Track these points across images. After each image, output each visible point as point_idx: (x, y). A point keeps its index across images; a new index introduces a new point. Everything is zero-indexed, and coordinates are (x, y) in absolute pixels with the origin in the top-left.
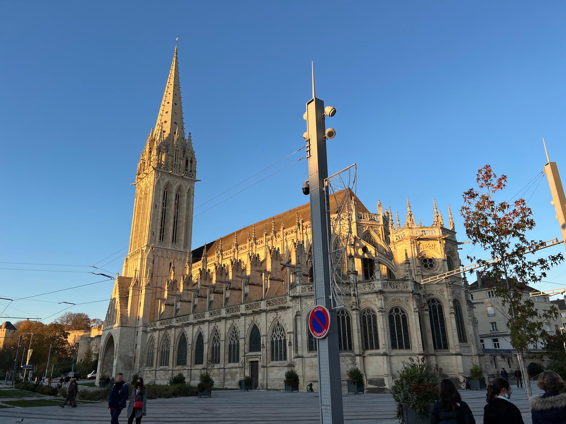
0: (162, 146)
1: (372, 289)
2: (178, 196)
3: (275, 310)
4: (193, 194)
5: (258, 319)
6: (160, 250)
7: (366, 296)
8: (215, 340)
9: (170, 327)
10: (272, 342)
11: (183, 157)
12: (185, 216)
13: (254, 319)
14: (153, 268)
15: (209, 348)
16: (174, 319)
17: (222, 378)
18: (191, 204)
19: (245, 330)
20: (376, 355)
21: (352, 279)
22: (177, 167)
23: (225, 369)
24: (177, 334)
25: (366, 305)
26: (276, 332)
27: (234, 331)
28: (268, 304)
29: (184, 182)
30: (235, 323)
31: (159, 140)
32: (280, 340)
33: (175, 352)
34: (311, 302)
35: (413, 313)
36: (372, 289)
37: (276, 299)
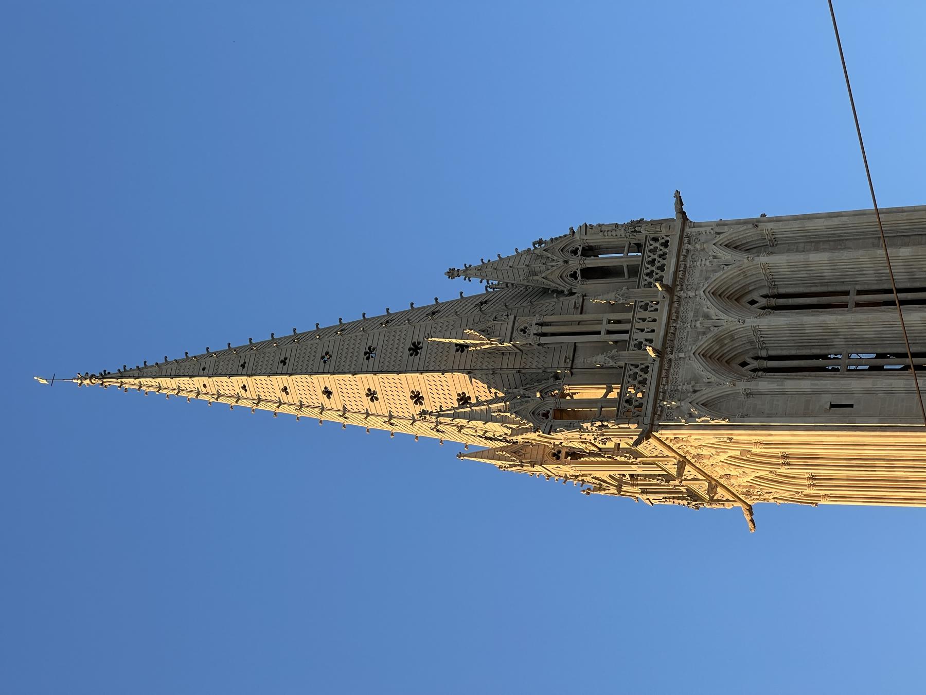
0: (531, 406)
2: (773, 301)
4: (755, 223)
11: (571, 293)
18: (810, 225)
22: (627, 321)
29: (695, 277)
31: (503, 421)
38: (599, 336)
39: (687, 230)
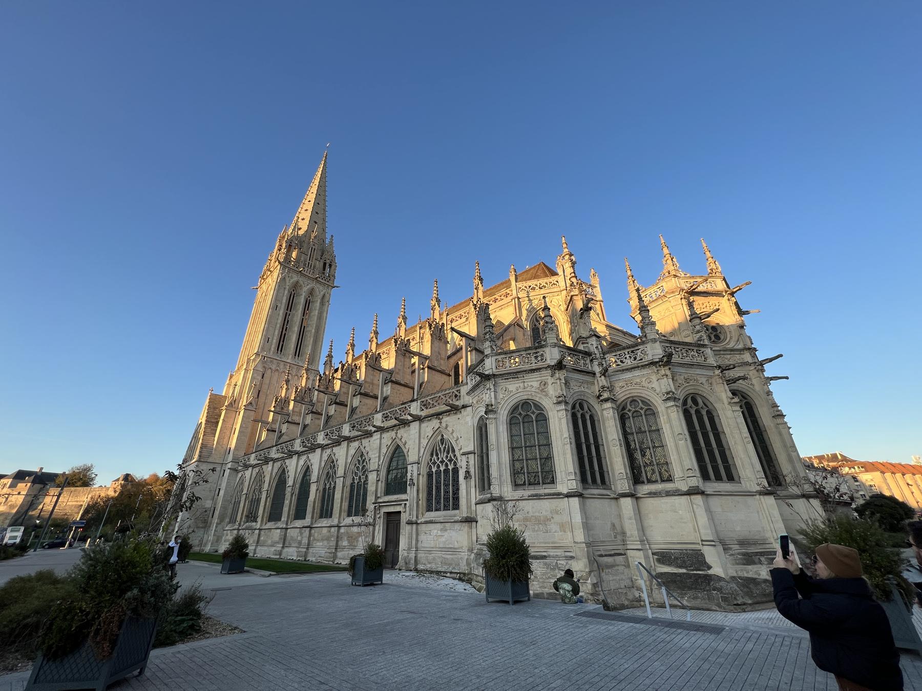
0: (294, 240)
1: (641, 359)
2: (308, 301)
3: (438, 415)
5: (405, 435)
6: (275, 361)
7: (628, 375)
8: (329, 477)
9: (267, 461)
10: (430, 475)
12: (315, 325)
13: (396, 436)
14: (261, 384)
15: (318, 491)
16: (275, 448)
17: (333, 543)
18: (325, 313)
19: (379, 457)
20: (669, 494)
21: (595, 346)
23: (339, 527)
24: (275, 471)
25: (627, 393)
26: (437, 455)
27: (361, 459)
28: (424, 405)
29: (318, 285)
30: (364, 445)
31: (292, 233)
32: (445, 470)
33: (268, 499)
34: (517, 385)
35: (727, 406)
36: (641, 359)
37: (440, 394)
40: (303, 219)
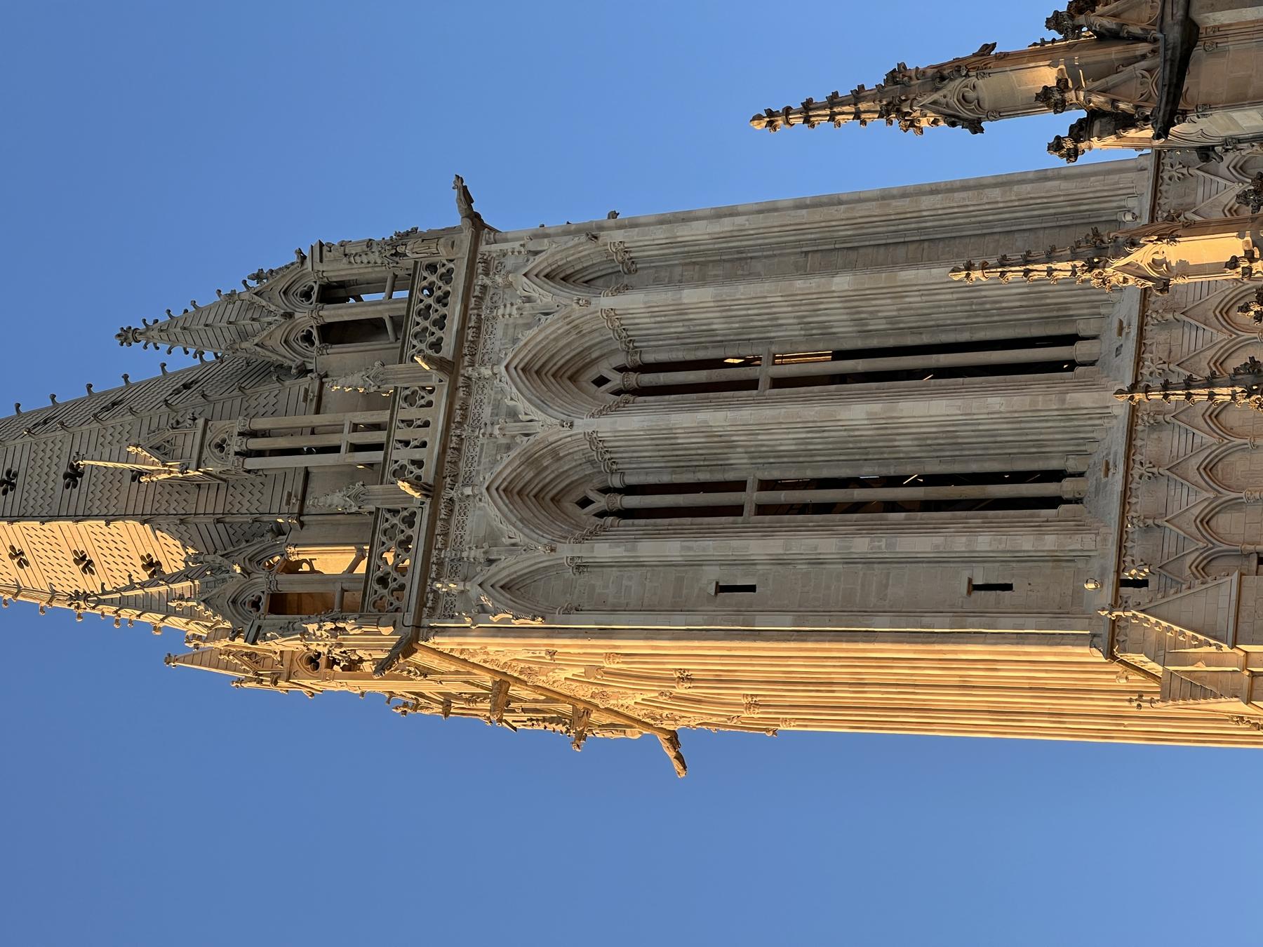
0: (230, 589)
2: (634, 379)
6: (1143, 502)
11: (303, 372)
12: (799, 284)
29: (496, 340)
31: (191, 615)
38: (336, 455)
39: (483, 248)
40: (85, 563)
